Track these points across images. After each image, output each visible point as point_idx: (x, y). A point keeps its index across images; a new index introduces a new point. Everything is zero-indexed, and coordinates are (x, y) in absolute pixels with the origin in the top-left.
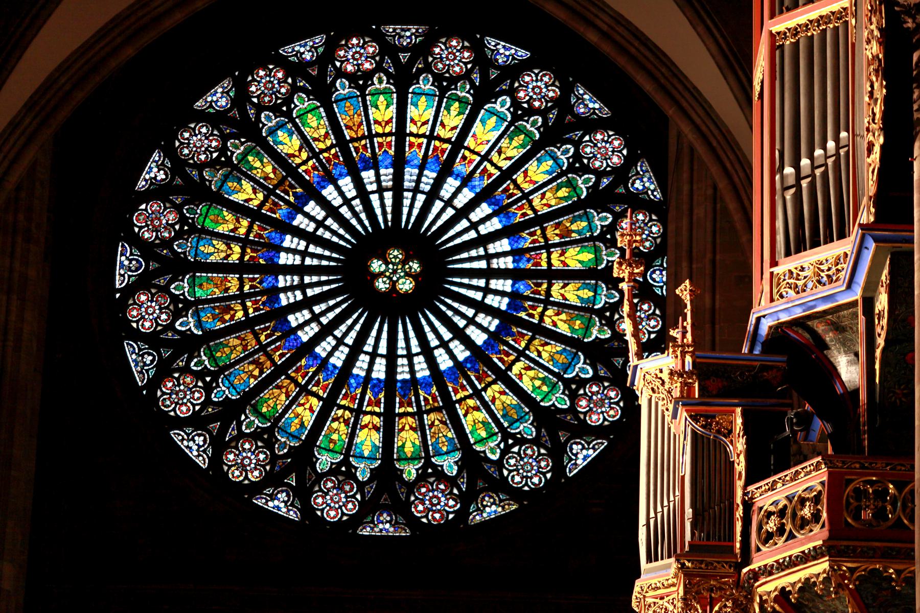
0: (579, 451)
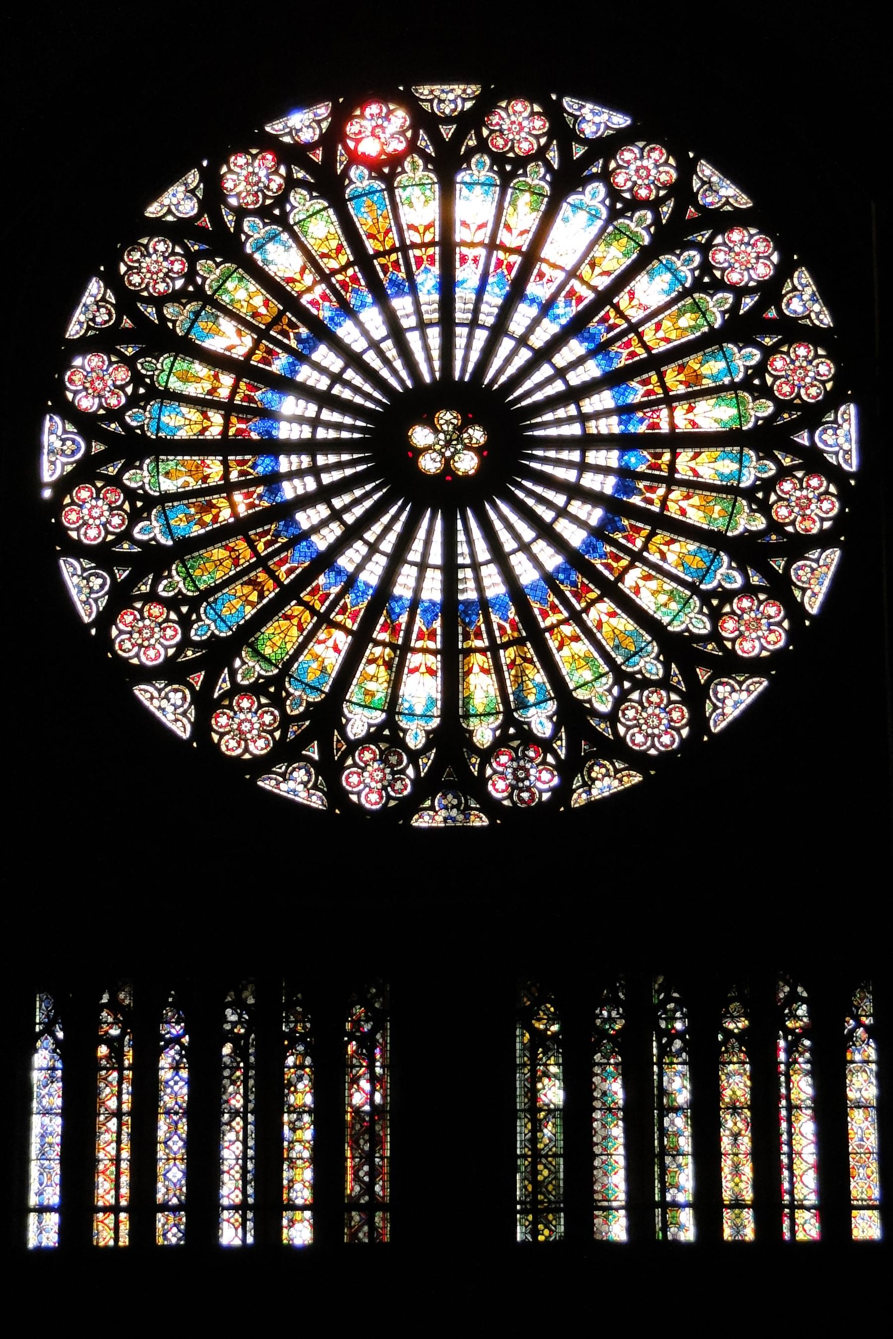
0: (727, 695)
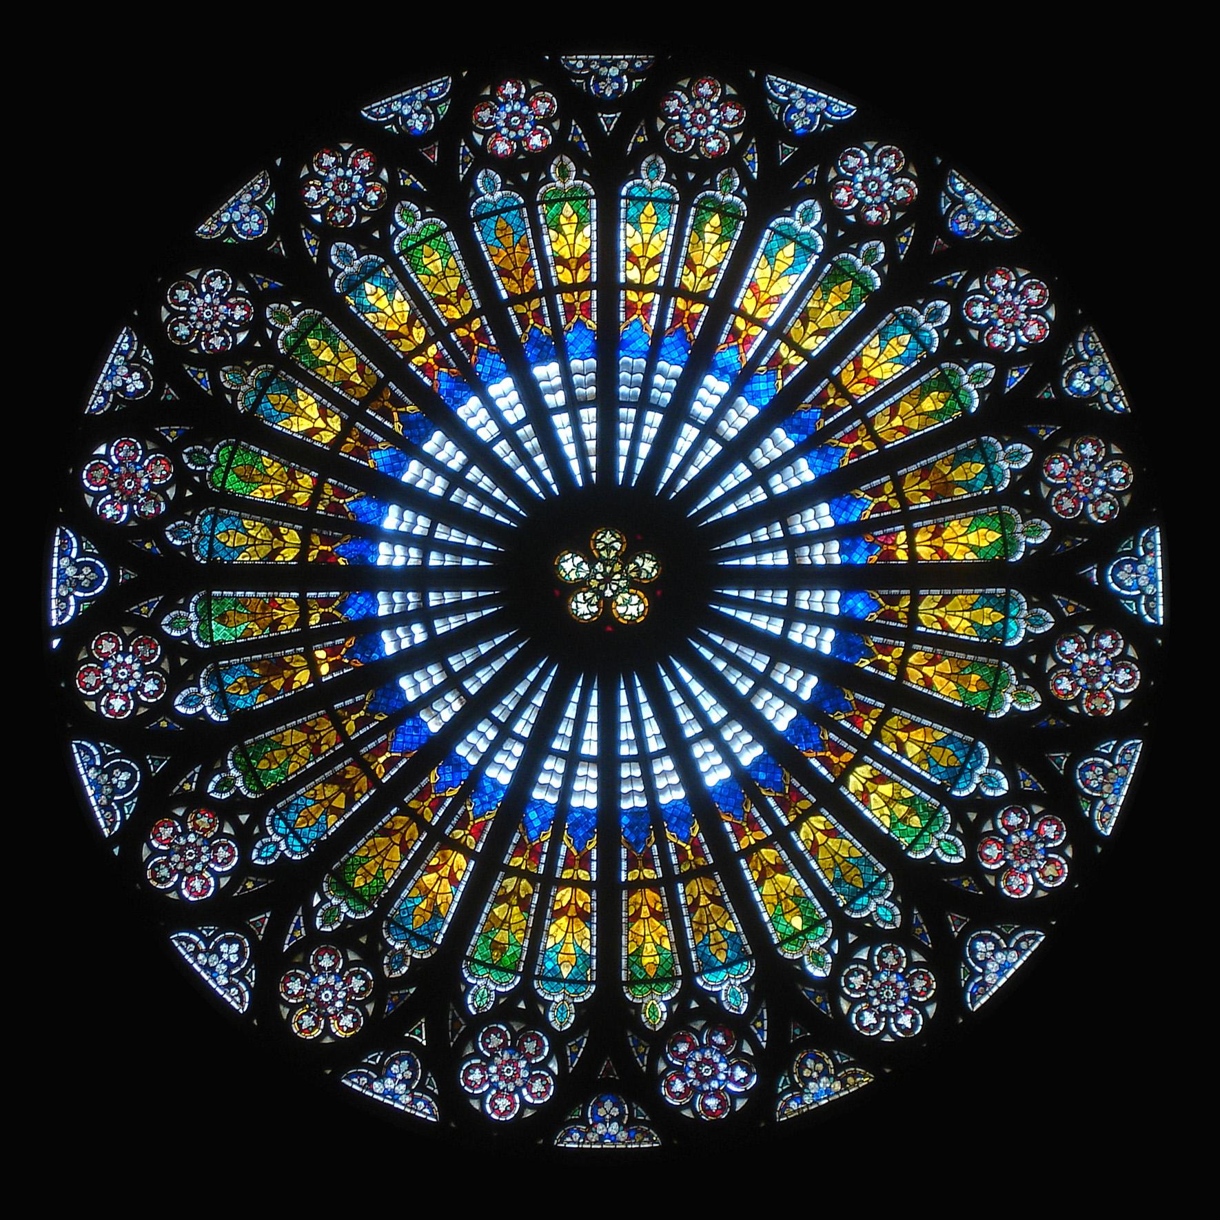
0: (989, 954)
